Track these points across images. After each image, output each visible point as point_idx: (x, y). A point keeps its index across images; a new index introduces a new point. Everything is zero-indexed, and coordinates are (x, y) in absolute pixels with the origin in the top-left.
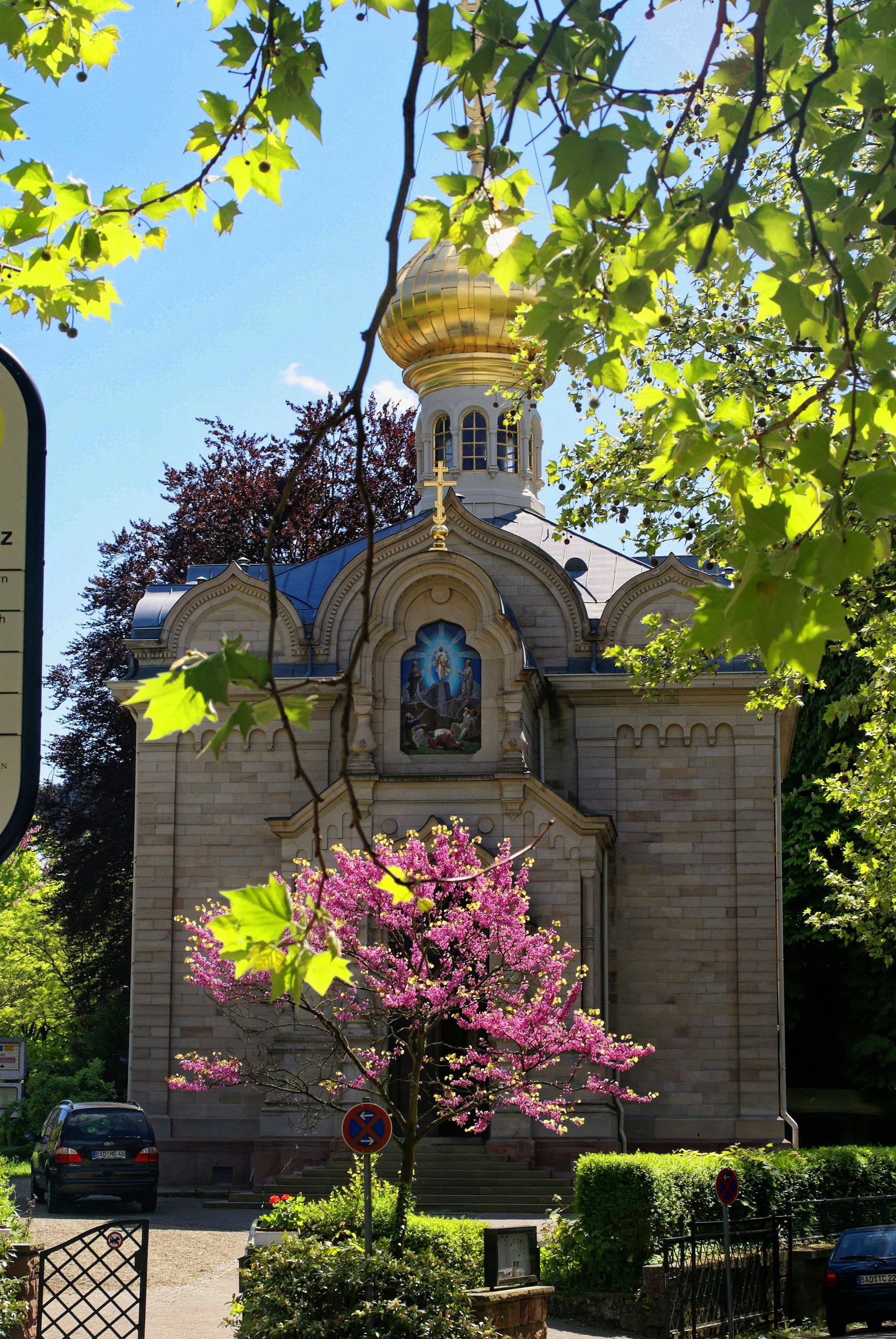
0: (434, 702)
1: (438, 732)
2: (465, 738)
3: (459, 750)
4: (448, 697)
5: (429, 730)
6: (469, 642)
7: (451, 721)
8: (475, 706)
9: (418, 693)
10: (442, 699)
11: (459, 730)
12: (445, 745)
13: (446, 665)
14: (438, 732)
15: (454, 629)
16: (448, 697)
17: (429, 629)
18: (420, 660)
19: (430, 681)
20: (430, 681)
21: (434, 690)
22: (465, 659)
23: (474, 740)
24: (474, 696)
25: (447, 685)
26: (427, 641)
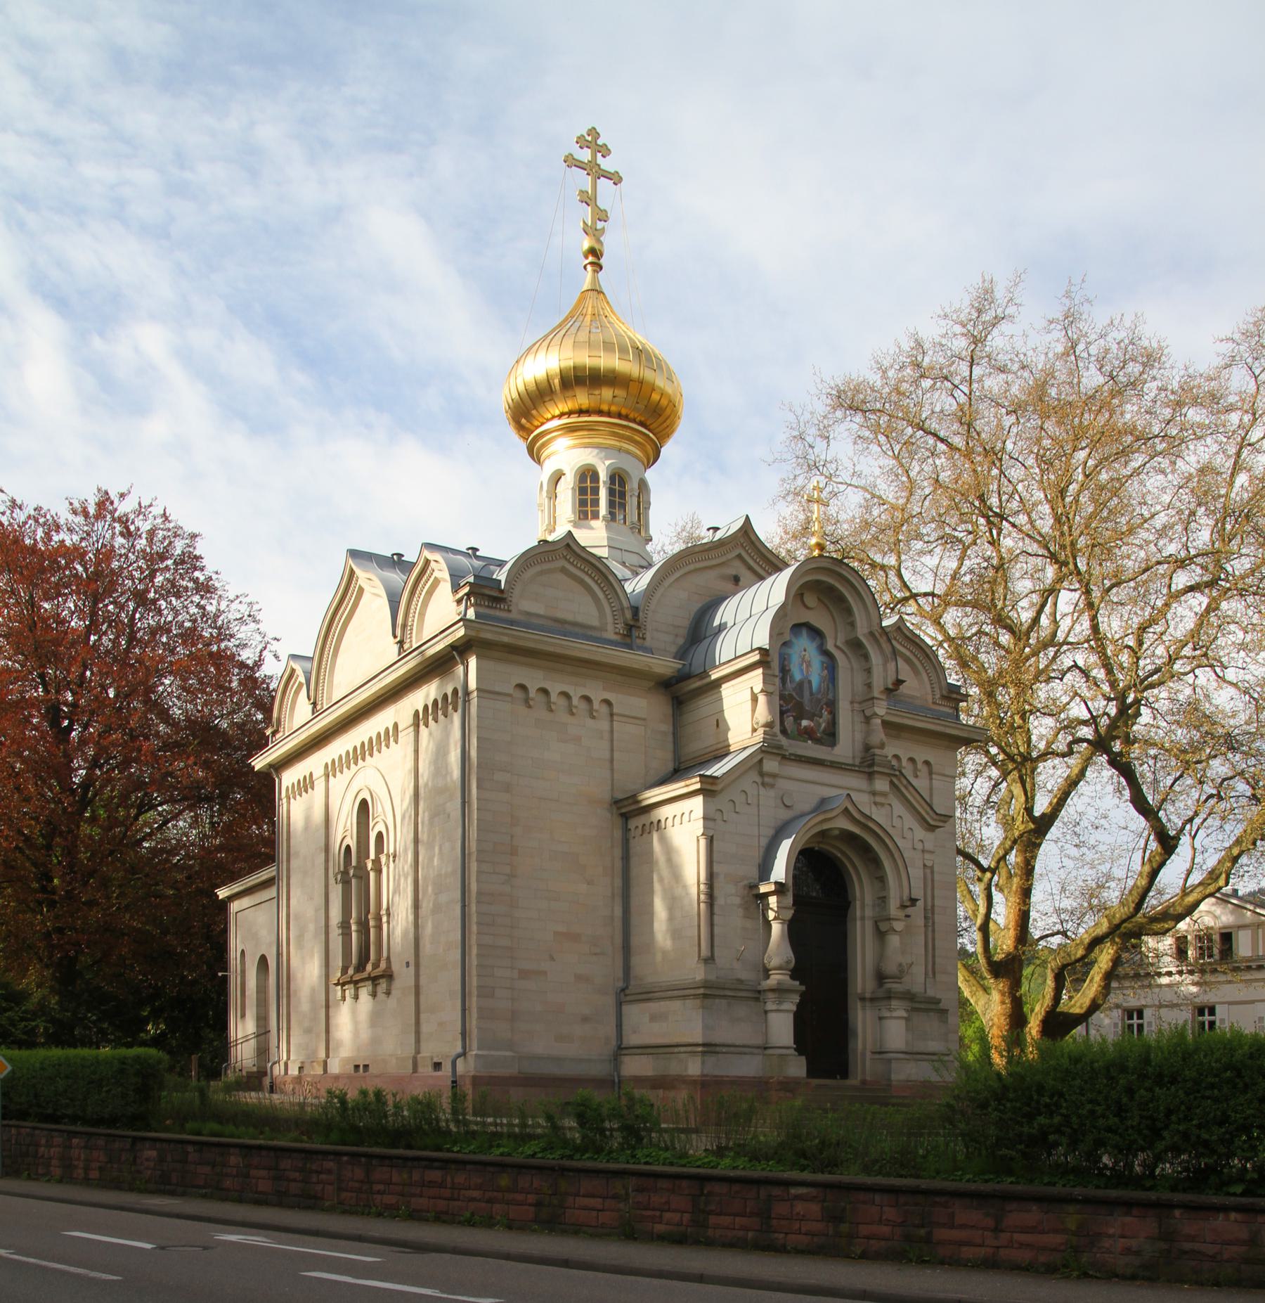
0: (802, 697)
1: (805, 723)
2: (824, 731)
3: (818, 741)
4: (811, 694)
5: (798, 719)
6: (830, 646)
7: (814, 715)
8: (832, 706)
9: (788, 684)
10: (806, 694)
11: (820, 725)
12: (809, 734)
13: (809, 665)
14: (805, 723)
15: (816, 633)
16: (811, 694)
17: (797, 628)
18: (789, 655)
19: (798, 677)
20: (798, 677)
21: (801, 684)
22: (823, 663)
23: (830, 736)
24: (830, 696)
25: (810, 682)
26: (794, 640)
